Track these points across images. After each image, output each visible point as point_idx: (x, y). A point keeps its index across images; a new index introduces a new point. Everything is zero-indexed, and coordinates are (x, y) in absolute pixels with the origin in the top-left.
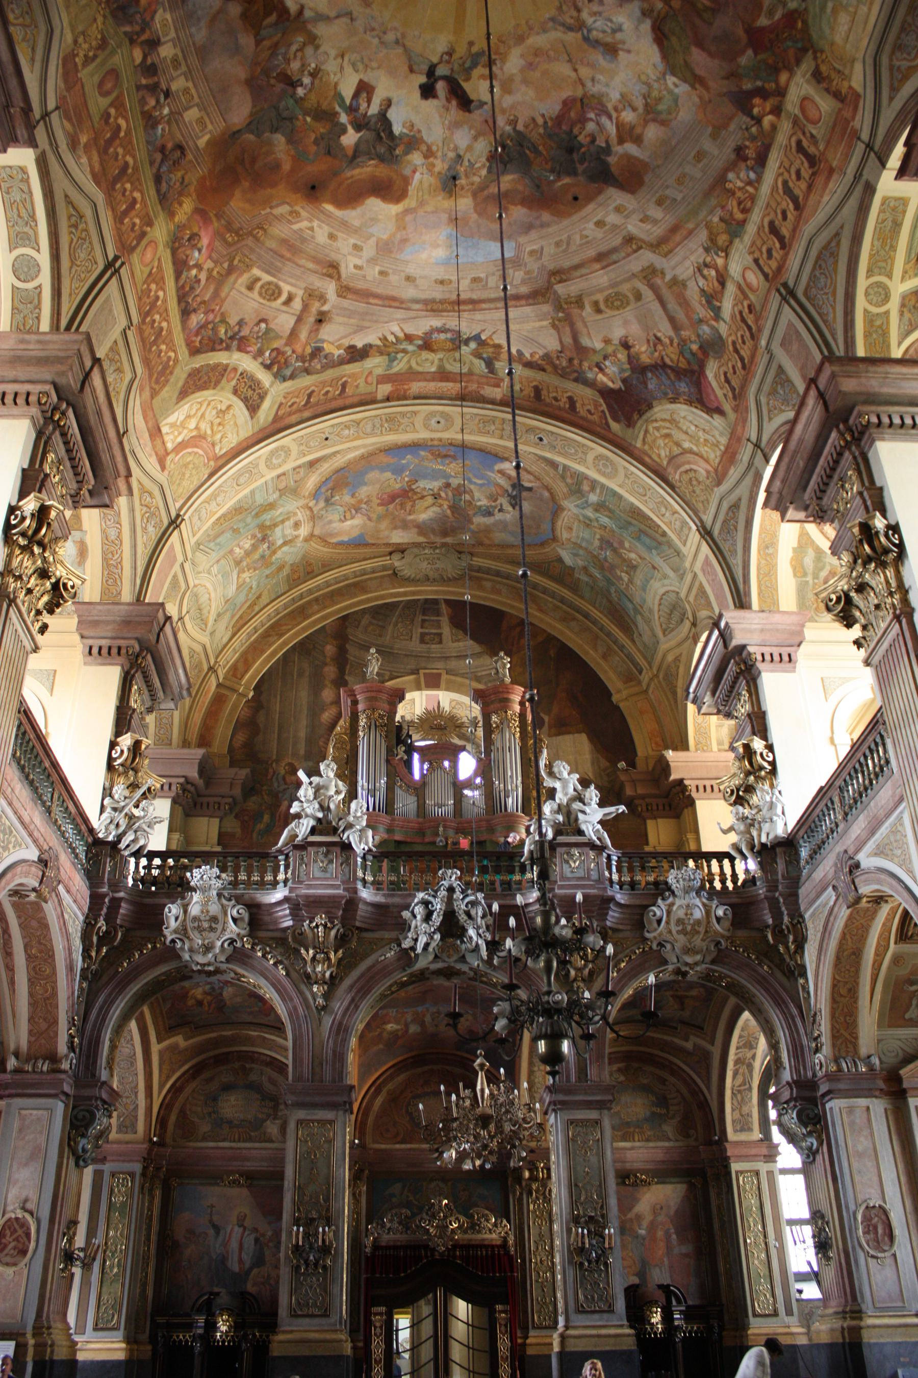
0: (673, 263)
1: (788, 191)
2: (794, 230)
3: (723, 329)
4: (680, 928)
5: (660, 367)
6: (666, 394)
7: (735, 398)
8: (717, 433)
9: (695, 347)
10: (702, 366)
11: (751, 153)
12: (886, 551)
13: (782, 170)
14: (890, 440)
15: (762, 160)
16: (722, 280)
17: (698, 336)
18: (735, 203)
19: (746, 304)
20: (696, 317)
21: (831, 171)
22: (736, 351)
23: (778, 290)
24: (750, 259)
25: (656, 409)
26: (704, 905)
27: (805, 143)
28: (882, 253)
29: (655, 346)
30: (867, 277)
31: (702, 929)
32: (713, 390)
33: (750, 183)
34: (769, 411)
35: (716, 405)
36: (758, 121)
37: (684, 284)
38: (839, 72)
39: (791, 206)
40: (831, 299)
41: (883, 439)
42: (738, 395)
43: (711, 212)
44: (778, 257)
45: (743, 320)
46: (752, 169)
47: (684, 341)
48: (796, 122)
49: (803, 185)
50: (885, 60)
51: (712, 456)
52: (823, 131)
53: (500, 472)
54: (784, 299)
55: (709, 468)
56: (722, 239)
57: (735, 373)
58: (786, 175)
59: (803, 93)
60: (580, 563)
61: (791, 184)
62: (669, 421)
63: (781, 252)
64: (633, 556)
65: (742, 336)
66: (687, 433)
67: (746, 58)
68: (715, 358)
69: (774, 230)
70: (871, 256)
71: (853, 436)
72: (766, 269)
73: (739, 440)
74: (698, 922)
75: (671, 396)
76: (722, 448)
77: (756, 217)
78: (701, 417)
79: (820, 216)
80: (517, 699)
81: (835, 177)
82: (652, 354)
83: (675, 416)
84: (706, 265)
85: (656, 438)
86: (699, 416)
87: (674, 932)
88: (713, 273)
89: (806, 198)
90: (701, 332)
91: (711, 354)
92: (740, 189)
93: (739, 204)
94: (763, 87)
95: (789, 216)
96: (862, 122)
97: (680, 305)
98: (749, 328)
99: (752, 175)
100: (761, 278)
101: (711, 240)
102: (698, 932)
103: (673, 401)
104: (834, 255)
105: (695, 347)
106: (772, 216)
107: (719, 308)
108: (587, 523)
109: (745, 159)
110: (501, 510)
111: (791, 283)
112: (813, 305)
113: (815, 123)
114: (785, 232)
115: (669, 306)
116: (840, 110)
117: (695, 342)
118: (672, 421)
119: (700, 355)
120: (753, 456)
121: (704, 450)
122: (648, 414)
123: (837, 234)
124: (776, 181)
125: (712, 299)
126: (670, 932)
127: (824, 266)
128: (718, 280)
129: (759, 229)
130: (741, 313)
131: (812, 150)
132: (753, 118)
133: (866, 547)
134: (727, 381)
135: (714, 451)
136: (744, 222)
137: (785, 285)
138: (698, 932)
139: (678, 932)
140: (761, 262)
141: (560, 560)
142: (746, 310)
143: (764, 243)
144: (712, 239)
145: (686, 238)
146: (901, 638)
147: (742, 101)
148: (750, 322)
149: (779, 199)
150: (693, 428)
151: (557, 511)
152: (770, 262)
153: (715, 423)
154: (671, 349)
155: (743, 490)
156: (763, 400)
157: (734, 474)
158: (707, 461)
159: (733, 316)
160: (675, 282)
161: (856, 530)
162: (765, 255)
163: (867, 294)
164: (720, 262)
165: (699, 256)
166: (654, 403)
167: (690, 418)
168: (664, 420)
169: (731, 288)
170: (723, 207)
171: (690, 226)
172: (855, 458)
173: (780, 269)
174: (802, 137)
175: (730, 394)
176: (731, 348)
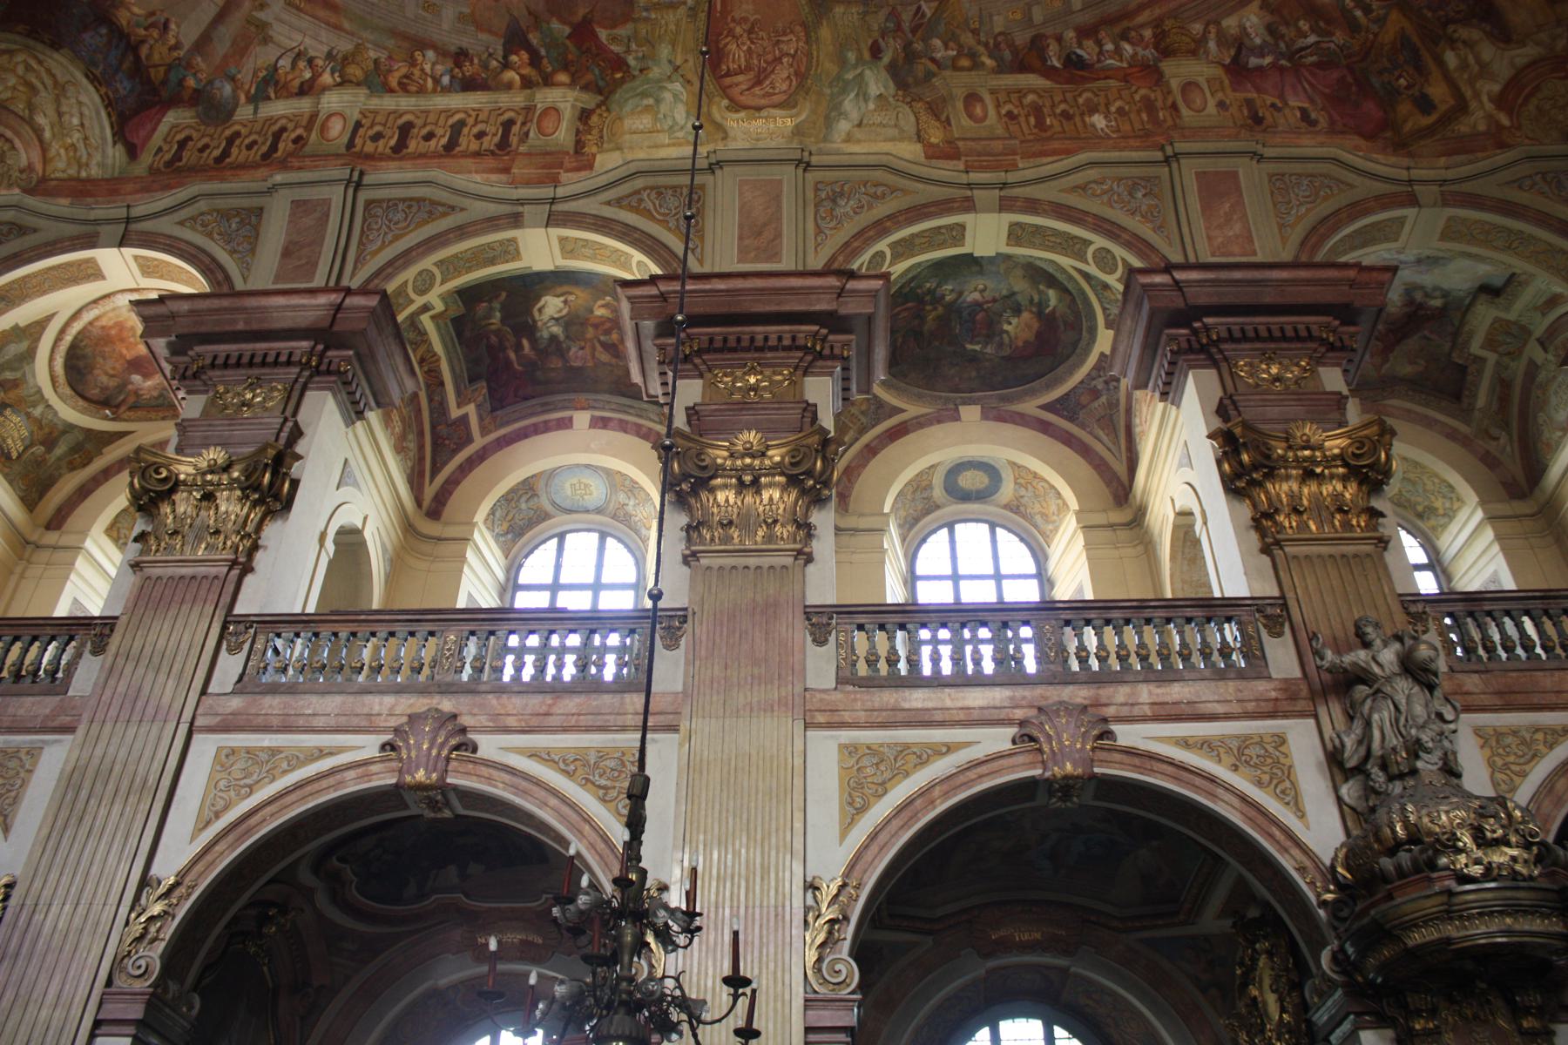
0: (285, 17)
1: (457, 128)
2: (422, 156)
3: (244, 112)
5: (128, 44)
6: (95, 65)
7: (169, 164)
8: (98, 157)
9: (191, 82)
10: (174, 102)
11: (469, 69)
12: (276, 497)
13: (474, 114)
14: (339, 404)
15: (469, 85)
16: (305, 90)
17: (210, 82)
18: (404, 71)
19: (299, 131)
20: (233, 71)
21: (506, 170)
22: (231, 141)
23: (352, 170)
24: (356, 116)
25: (56, 56)
27: (515, 129)
28: (462, 263)
29: (153, 25)
30: (435, 264)
32: (154, 129)
33: (436, 81)
34: (194, 219)
35: (135, 141)
36: (506, 65)
37: (267, 40)
38: (601, 137)
39: (444, 141)
40: (390, 237)
41: (335, 396)
42: (174, 170)
43: (377, 45)
44: (380, 149)
45: (277, 136)
46: (453, 77)
47: (189, 66)
48: (529, 109)
49: (474, 146)
50: (639, 183)
51: (61, 165)
52: (538, 143)
54: (349, 181)
55: (39, 167)
56: (355, 71)
57: (201, 150)
58: (471, 121)
59: (561, 106)
61: (465, 130)
62: (56, 83)
63: (388, 151)
65: (255, 142)
66: (60, 115)
67: (560, 29)
68: (198, 116)
69: (405, 130)
70: (456, 256)
71: (319, 364)
72: (358, 141)
73: (114, 192)
75: (97, 72)
76: (84, 174)
77: (405, 103)
78: (102, 128)
79: (460, 181)
81: (503, 177)
82: (138, 25)
83: (71, 90)
84: (310, 61)
85: (14, 71)
86: (101, 126)
88: (308, 75)
89: (465, 155)
90: (217, 84)
91: (200, 108)
92: (422, 70)
93: (406, 76)
94: (542, 58)
95: (433, 142)
96: (572, 183)
97: (234, 43)
98: (274, 148)
99: (446, 80)
100: (345, 139)
101: (345, 58)
103: (93, 79)
104: (432, 216)
105: (191, 82)
106: (419, 122)
107: (268, 98)
109: (458, 65)
111: (367, 179)
112: (364, 220)
113: (540, 131)
114: (413, 145)
115: (222, 29)
116: (568, 153)
117: (199, 81)
118: (60, 90)
119: (186, 95)
120: (109, 221)
121: (55, 147)
122: (40, 46)
123: (453, 208)
124: (458, 111)
125: (270, 85)
127: (414, 210)
128: (302, 84)
129: (394, 112)
130: (283, 130)
131: (514, 140)
132: (505, 57)
133: (267, 476)
134: (182, 144)
135: (69, 164)
136: (391, 91)
137: (362, 174)
140: (361, 131)
142: (293, 136)
143: (384, 125)
144: (346, 60)
145: (328, 24)
146: (217, 584)
147: (515, 40)
148: (281, 146)
149: (441, 122)
150: (76, 121)
152: (368, 142)
153: (110, 150)
154: (165, 50)
155: (52, 230)
156: (202, 205)
157: (62, 205)
158: (45, 160)
159: (271, 121)
160: (262, 26)
161: (271, 452)
162: (371, 133)
163: (420, 273)
164: (327, 78)
165: (318, 50)
166: (65, 51)
167: (86, 112)
168: (53, 76)
169: (305, 105)
170: (390, 58)
171: (347, 25)
172: (296, 381)
173: (370, 157)
174: (519, 123)
175: (168, 157)
176: (228, 133)
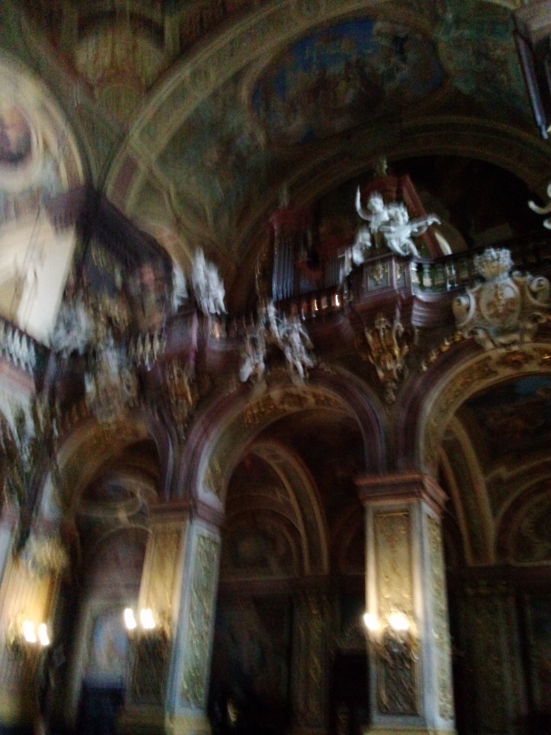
4: (492, 311)
26: (517, 283)
31: (517, 308)
53: (379, 33)
60: (473, 86)
64: (499, 52)
74: (511, 301)
80: (394, 189)
87: (487, 318)
102: (512, 311)
108: (458, 44)
110: (398, 70)
126: (482, 317)
138: (512, 311)
139: (491, 316)
141: (459, 93)
151: (434, 45)
